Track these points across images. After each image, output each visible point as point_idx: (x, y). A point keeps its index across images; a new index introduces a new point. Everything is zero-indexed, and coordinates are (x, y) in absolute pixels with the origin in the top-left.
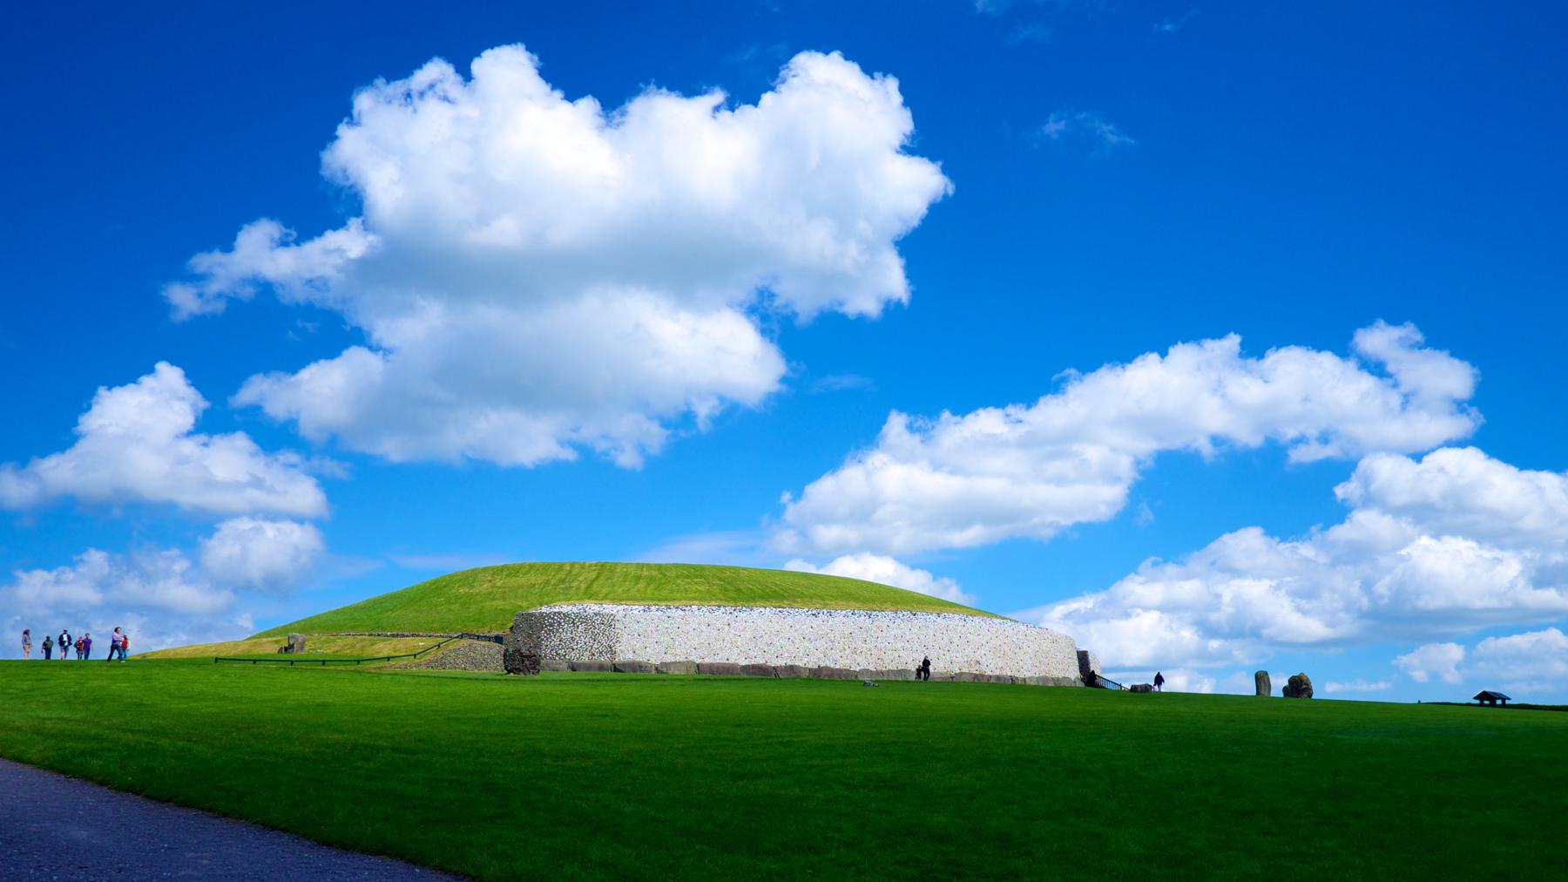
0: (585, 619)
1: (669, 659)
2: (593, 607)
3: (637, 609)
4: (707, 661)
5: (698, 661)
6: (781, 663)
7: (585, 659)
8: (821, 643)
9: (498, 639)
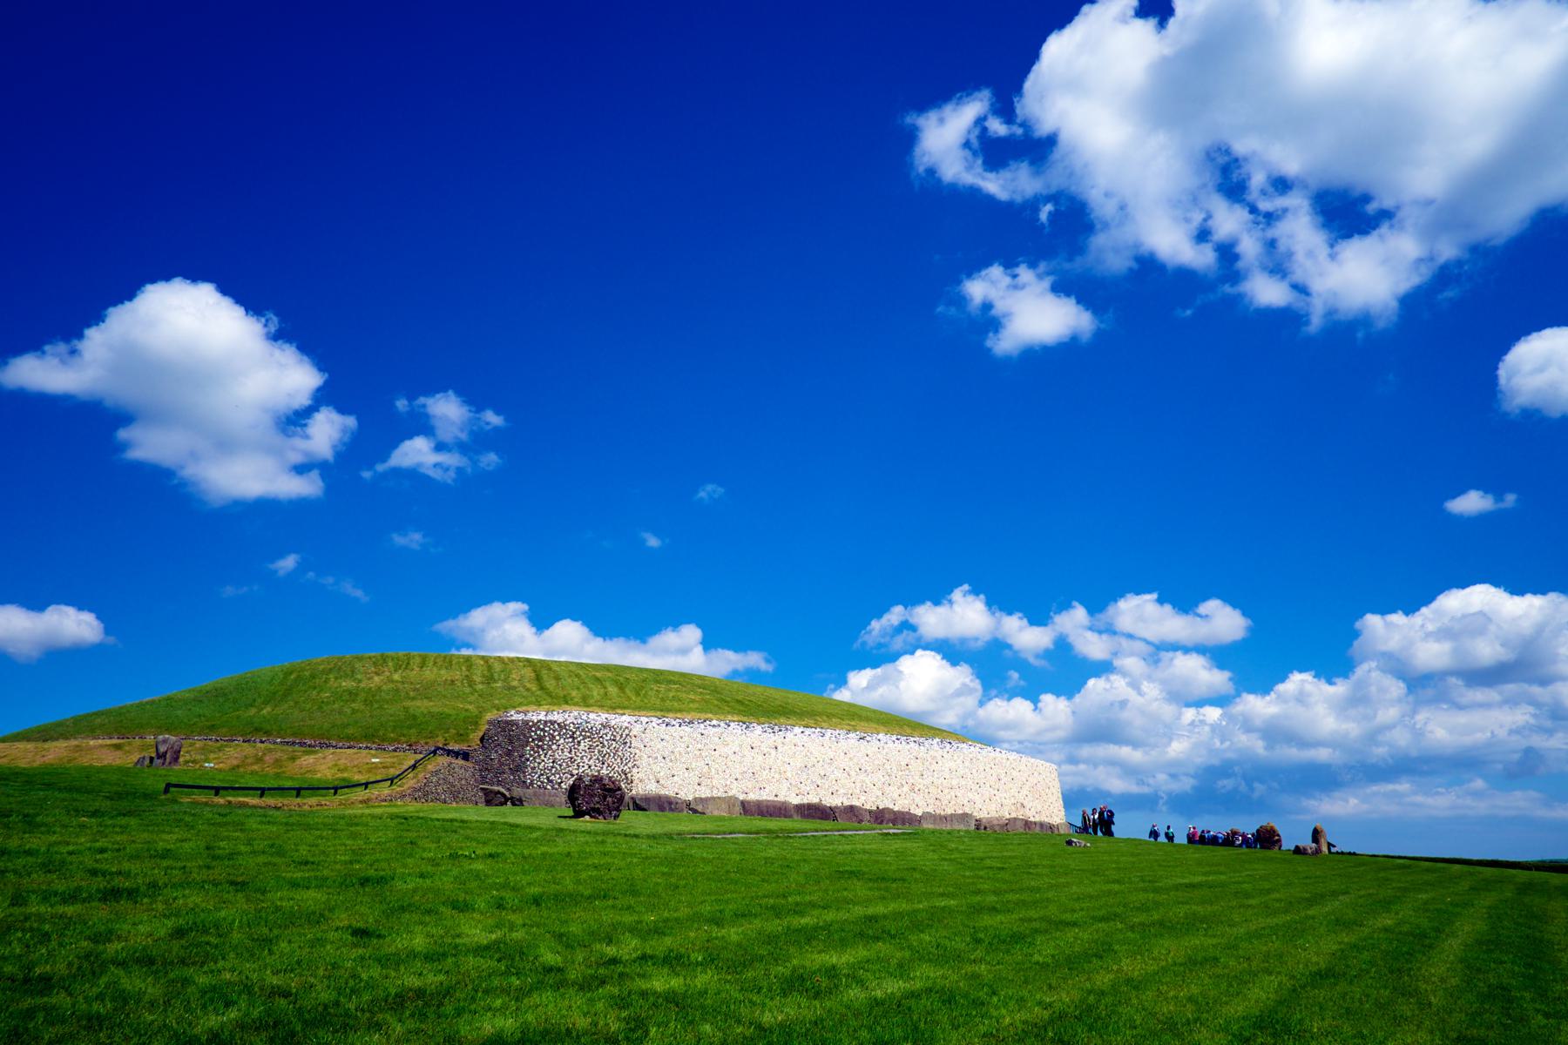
0: (590, 733)
1: (704, 793)
2: (597, 718)
4: (753, 796)
8: (879, 777)
9: (466, 756)
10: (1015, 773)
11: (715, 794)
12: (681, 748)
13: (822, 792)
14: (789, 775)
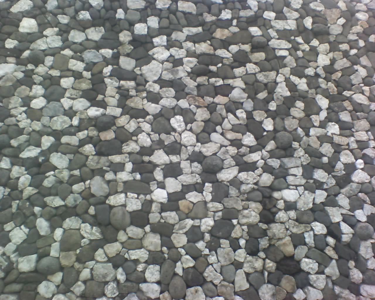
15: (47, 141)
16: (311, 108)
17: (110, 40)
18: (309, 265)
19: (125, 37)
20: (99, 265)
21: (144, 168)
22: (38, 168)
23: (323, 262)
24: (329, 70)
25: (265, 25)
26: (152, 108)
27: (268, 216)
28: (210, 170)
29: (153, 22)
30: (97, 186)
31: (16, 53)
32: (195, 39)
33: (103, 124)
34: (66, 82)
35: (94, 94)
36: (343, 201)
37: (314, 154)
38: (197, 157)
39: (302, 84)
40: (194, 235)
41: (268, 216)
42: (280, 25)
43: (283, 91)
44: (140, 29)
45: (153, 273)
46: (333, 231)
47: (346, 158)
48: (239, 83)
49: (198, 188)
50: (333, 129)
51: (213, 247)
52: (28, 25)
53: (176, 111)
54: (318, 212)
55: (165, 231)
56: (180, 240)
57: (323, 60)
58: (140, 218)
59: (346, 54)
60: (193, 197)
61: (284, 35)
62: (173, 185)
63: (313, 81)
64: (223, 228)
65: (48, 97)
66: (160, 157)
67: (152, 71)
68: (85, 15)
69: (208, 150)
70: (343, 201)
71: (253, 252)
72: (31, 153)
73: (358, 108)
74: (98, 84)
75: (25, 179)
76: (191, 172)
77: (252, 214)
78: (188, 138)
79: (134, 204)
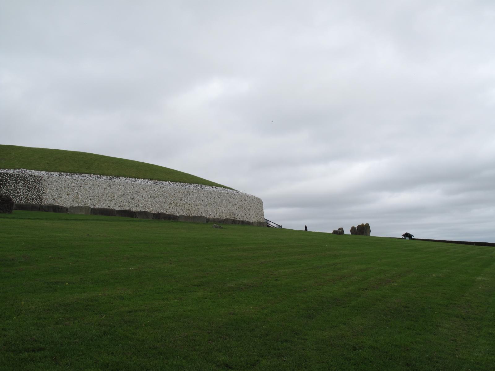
0: (24, 179)
1: (75, 204)
3: (55, 174)
4: (97, 207)
5: (92, 207)
6: (138, 209)
7: (23, 202)
10: (231, 200)
11: (80, 205)
12: (65, 185)
13: (131, 206)
14: (116, 198)
15: (11, 190)
16: (32, 188)
17: (16, 182)
18: (30, 200)
19: (17, 182)
20: (15, 199)
21: (18, 192)
22: (10, 192)
23: (31, 200)
24: (35, 185)
25: (29, 181)
26: (19, 188)
27: (27, 196)
28: (23, 193)
29: (20, 180)
30: (15, 194)
31: (8, 183)
32: (23, 182)
33: (15, 189)
34: (12, 185)
35: (14, 187)
36: (33, 196)
37: (32, 192)
38: (22, 192)
39: (32, 186)
40: (21, 197)
41: (27, 196)
42: (31, 181)
43: (30, 187)
44: (19, 181)
45: (18, 200)
46: (32, 198)
47: (34, 192)
48: (26, 186)
49: (22, 194)
50: (34, 190)
51: (23, 198)
52: (9, 180)
53: (21, 188)
54: (31, 196)
55: (19, 197)
56: (20, 198)
57: (34, 184)
58: (17, 196)
59: (37, 184)
60: (22, 195)
61: (31, 182)
62: (20, 194)
63: (33, 186)
64: (24, 197)
65: (11, 187)
66: (19, 192)
67: (19, 185)
68: (14, 180)
69: (23, 191)
70: (33, 196)
71: (26, 198)
72: (9, 191)
73: (36, 188)
74: (15, 186)
75: (9, 193)
76: (22, 193)
77: (26, 196)
78: (22, 190)
79: (17, 195)
